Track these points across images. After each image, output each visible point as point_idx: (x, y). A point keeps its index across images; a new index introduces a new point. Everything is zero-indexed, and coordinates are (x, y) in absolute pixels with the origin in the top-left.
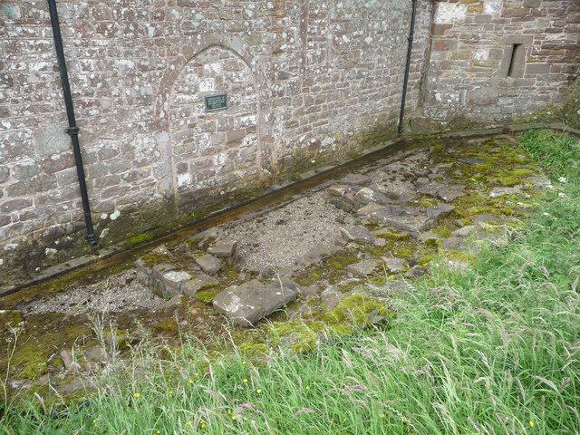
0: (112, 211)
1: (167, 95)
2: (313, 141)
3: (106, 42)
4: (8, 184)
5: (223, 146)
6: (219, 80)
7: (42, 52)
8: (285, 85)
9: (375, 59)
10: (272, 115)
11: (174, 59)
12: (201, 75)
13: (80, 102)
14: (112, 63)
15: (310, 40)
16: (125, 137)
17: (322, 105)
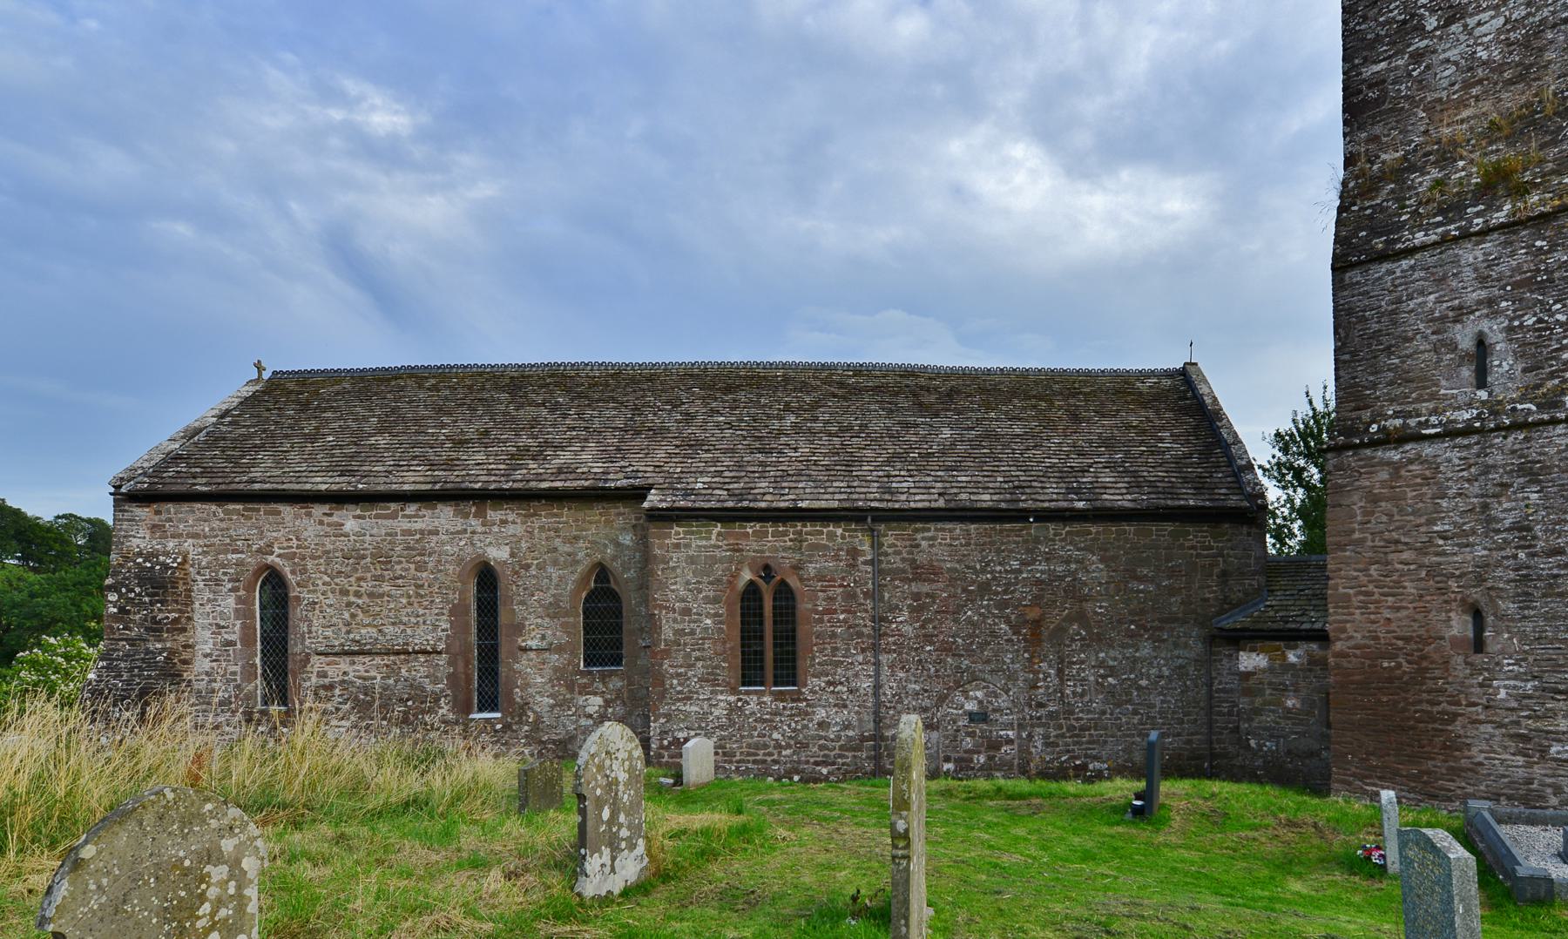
6: (980, 702)
8: (1042, 712)
9: (1157, 700)
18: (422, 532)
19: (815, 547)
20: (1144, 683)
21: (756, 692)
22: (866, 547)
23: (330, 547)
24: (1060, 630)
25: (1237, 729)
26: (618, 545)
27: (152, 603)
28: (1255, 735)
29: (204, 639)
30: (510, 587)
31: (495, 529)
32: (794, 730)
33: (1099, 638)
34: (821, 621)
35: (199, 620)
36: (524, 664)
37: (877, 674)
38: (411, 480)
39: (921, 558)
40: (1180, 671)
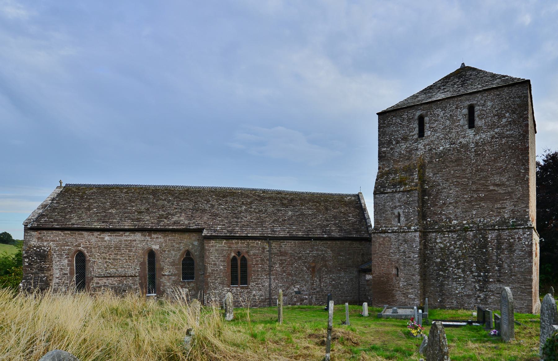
8: (315, 291)
18: (131, 240)
19: (252, 247)
22: (267, 247)
23: (100, 245)
24: (320, 269)
25: (365, 295)
26: (193, 245)
27: (40, 262)
29: (56, 273)
30: (159, 257)
31: (155, 240)
34: (254, 267)
35: (54, 267)
36: (163, 280)
37: (270, 281)
38: (127, 225)
39: (282, 250)
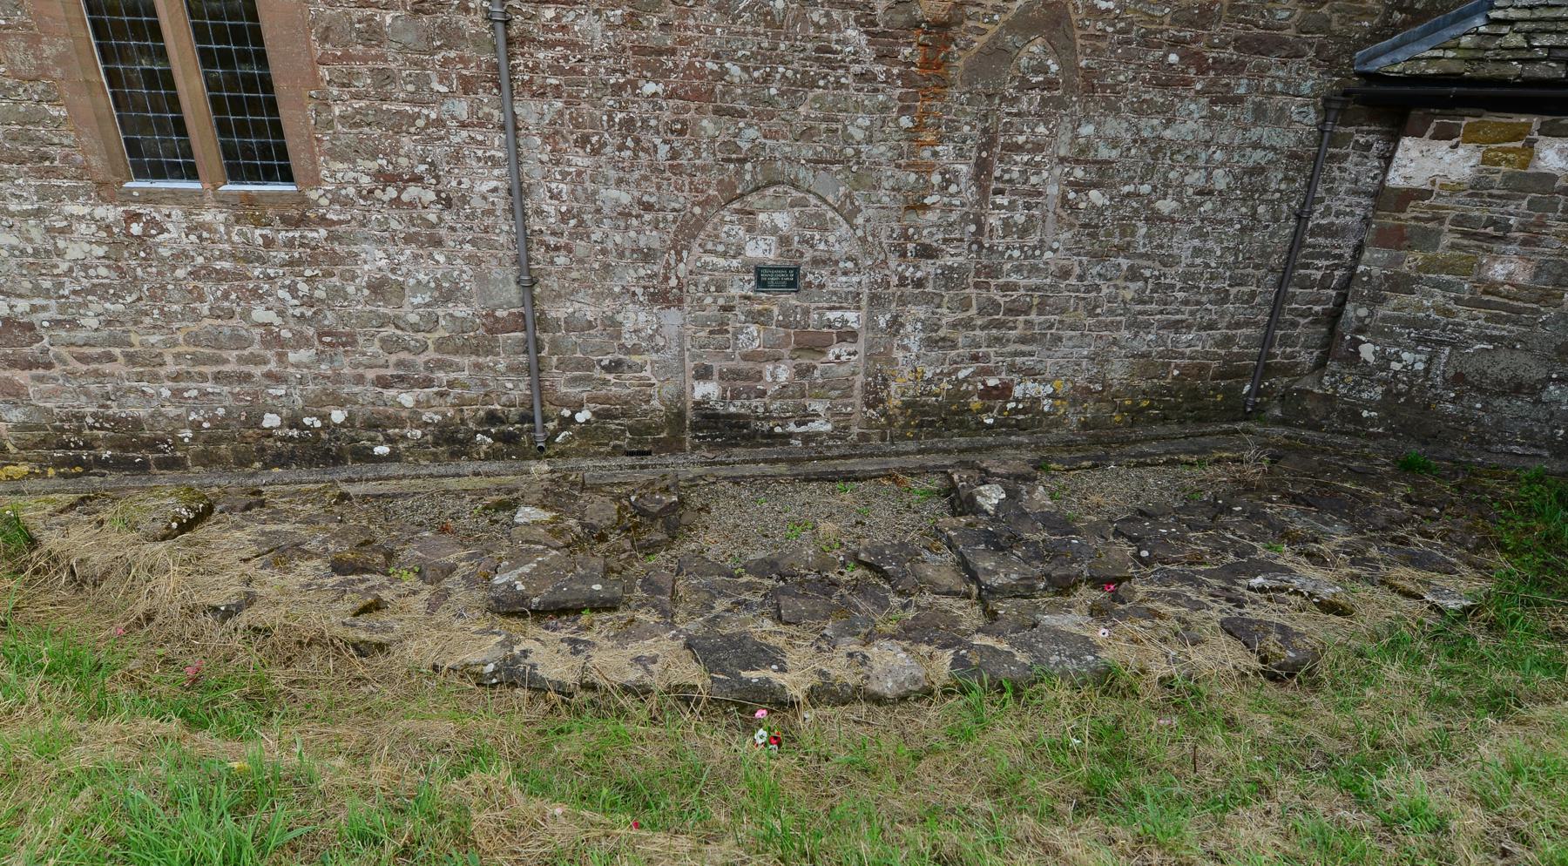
0: (579, 407)
1: (685, 254)
2: (992, 382)
3: (587, 162)
4: (436, 335)
5: (786, 352)
6: (784, 241)
7: (494, 166)
8: (928, 268)
9: (1183, 246)
10: (895, 319)
11: (701, 198)
12: (750, 230)
13: (542, 243)
14: (595, 193)
15: (1001, 192)
16: (608, 306)
17: (1021, 318)
20: (1166, 206)
21: (175, 197)
24: (998, 54)
28: (1378, 333)
32: (309, 301)
33: (1090, 84)
37: (516, 158)
40: (1251, 181)
